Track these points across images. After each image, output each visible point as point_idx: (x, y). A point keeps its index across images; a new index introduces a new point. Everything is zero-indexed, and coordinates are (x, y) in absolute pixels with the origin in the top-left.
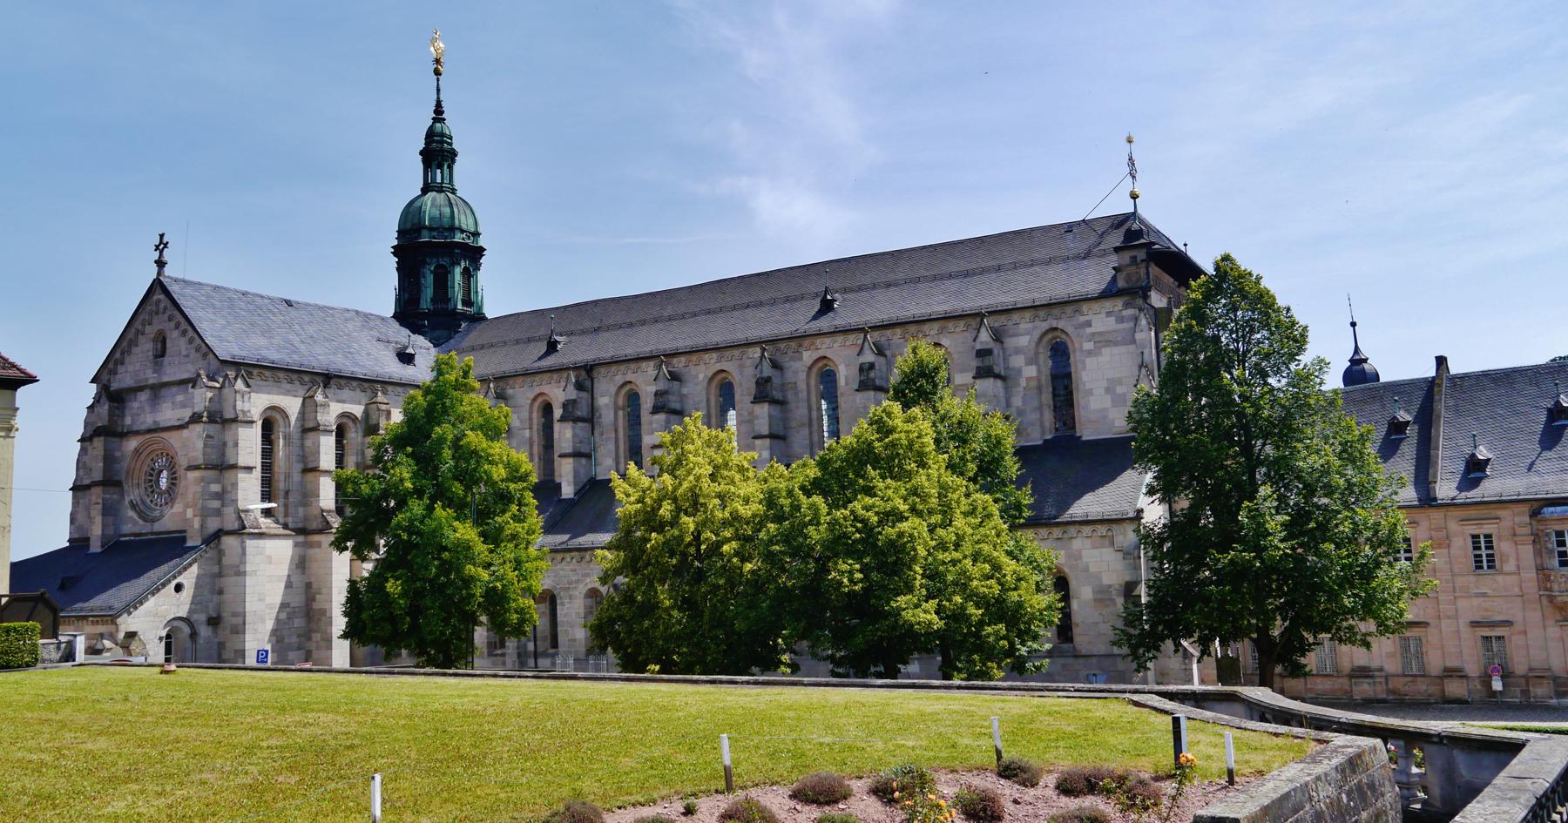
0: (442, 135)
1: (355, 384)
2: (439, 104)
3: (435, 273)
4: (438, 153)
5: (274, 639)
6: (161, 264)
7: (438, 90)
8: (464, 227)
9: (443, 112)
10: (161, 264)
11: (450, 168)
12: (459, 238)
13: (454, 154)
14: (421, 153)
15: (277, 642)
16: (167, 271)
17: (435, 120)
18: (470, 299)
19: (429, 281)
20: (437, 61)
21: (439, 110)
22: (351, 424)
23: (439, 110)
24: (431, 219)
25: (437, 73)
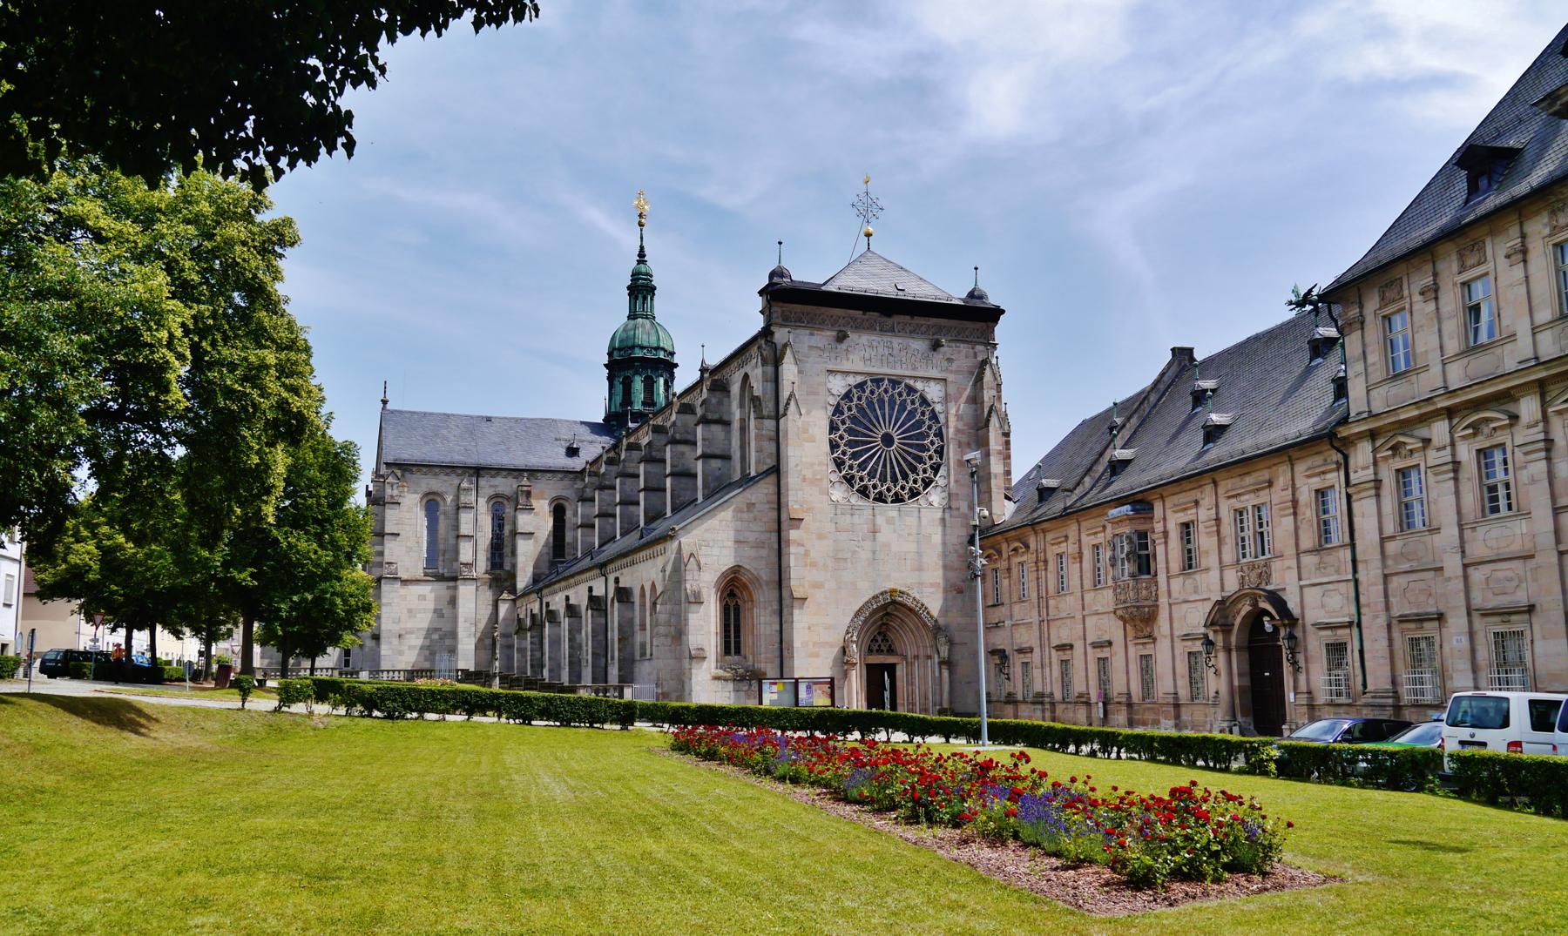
0: (647, 274)
1: (504, 473)
2: (642, 248)
3: (622, 383)
4: (641, 289)
5: (427, 652)
6: (385, 402)
7: (642, 238)
8: (645, 344)
9: (644, 256)
10: (385, 402)
11: (652, 299)
12: (638, 353)
13: (654, 288)
14: (628, 288)
15: (430, 654)
16: (389, 406)
17: (639, 262)
18: (653, 400)
19: (619, 388)
20: (641, 216)
21: (642, 254)
22: (505, 502)
23: (642, 254)
24: (620, 342)
25: (641, 225)
